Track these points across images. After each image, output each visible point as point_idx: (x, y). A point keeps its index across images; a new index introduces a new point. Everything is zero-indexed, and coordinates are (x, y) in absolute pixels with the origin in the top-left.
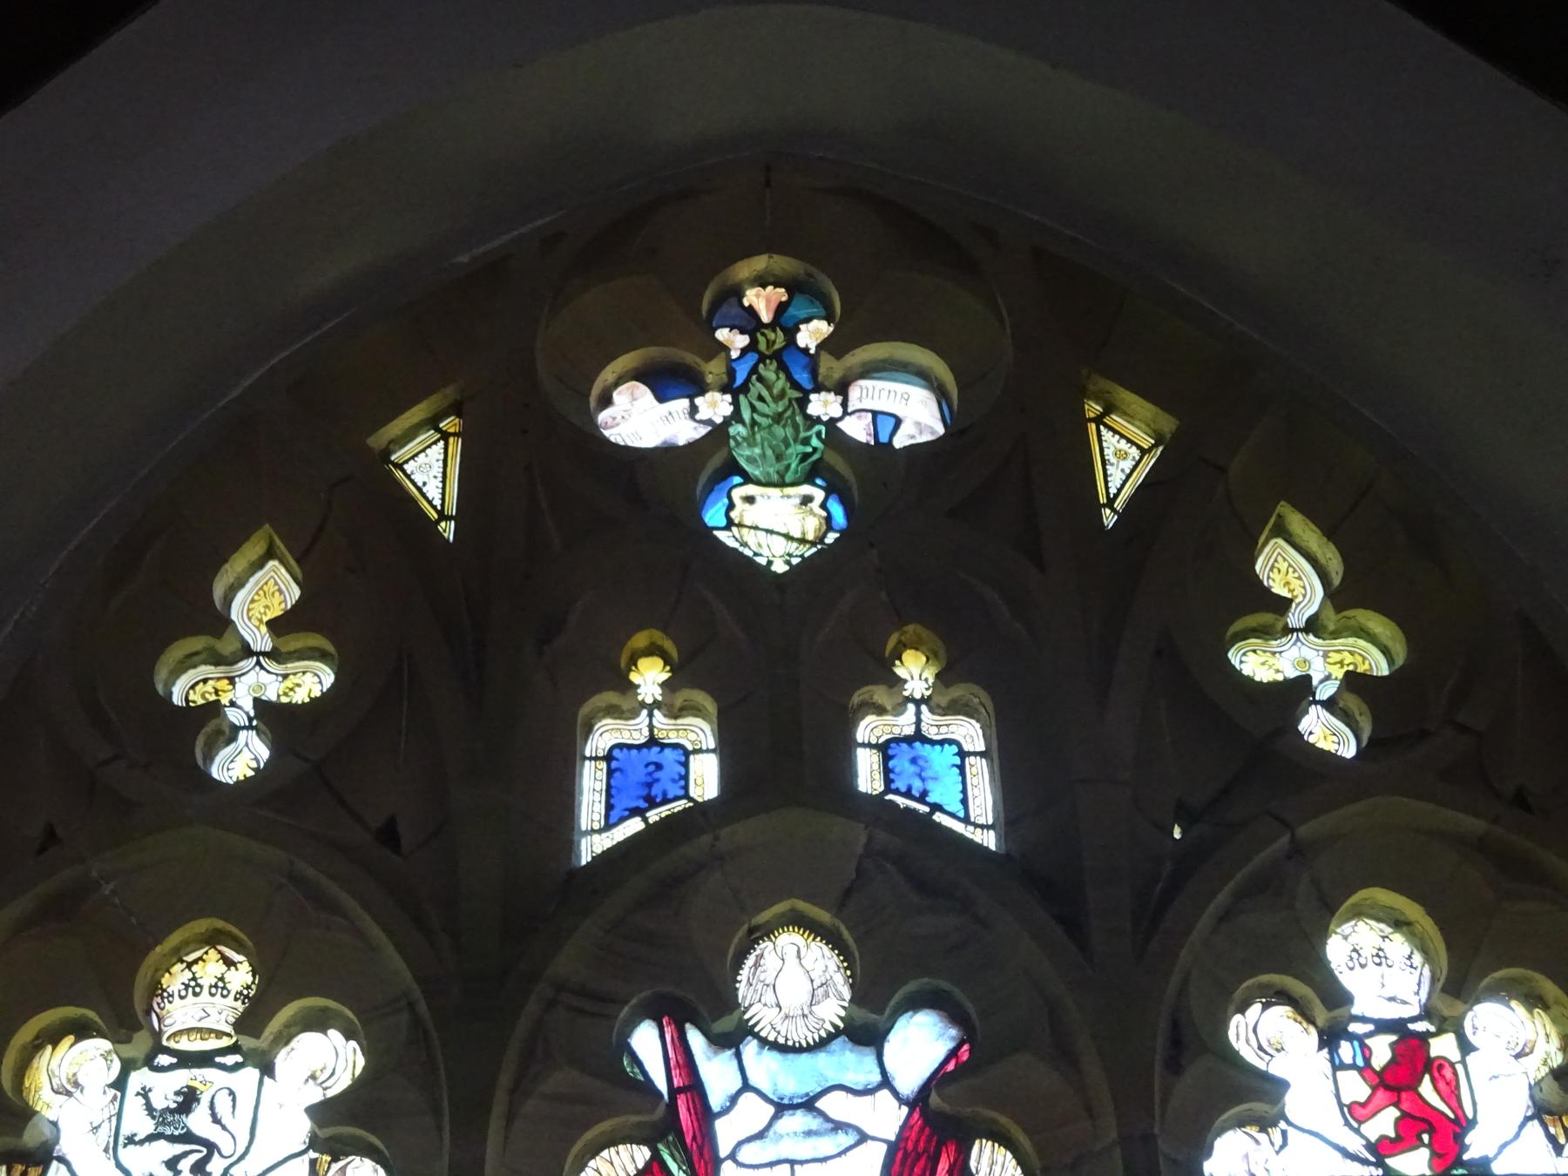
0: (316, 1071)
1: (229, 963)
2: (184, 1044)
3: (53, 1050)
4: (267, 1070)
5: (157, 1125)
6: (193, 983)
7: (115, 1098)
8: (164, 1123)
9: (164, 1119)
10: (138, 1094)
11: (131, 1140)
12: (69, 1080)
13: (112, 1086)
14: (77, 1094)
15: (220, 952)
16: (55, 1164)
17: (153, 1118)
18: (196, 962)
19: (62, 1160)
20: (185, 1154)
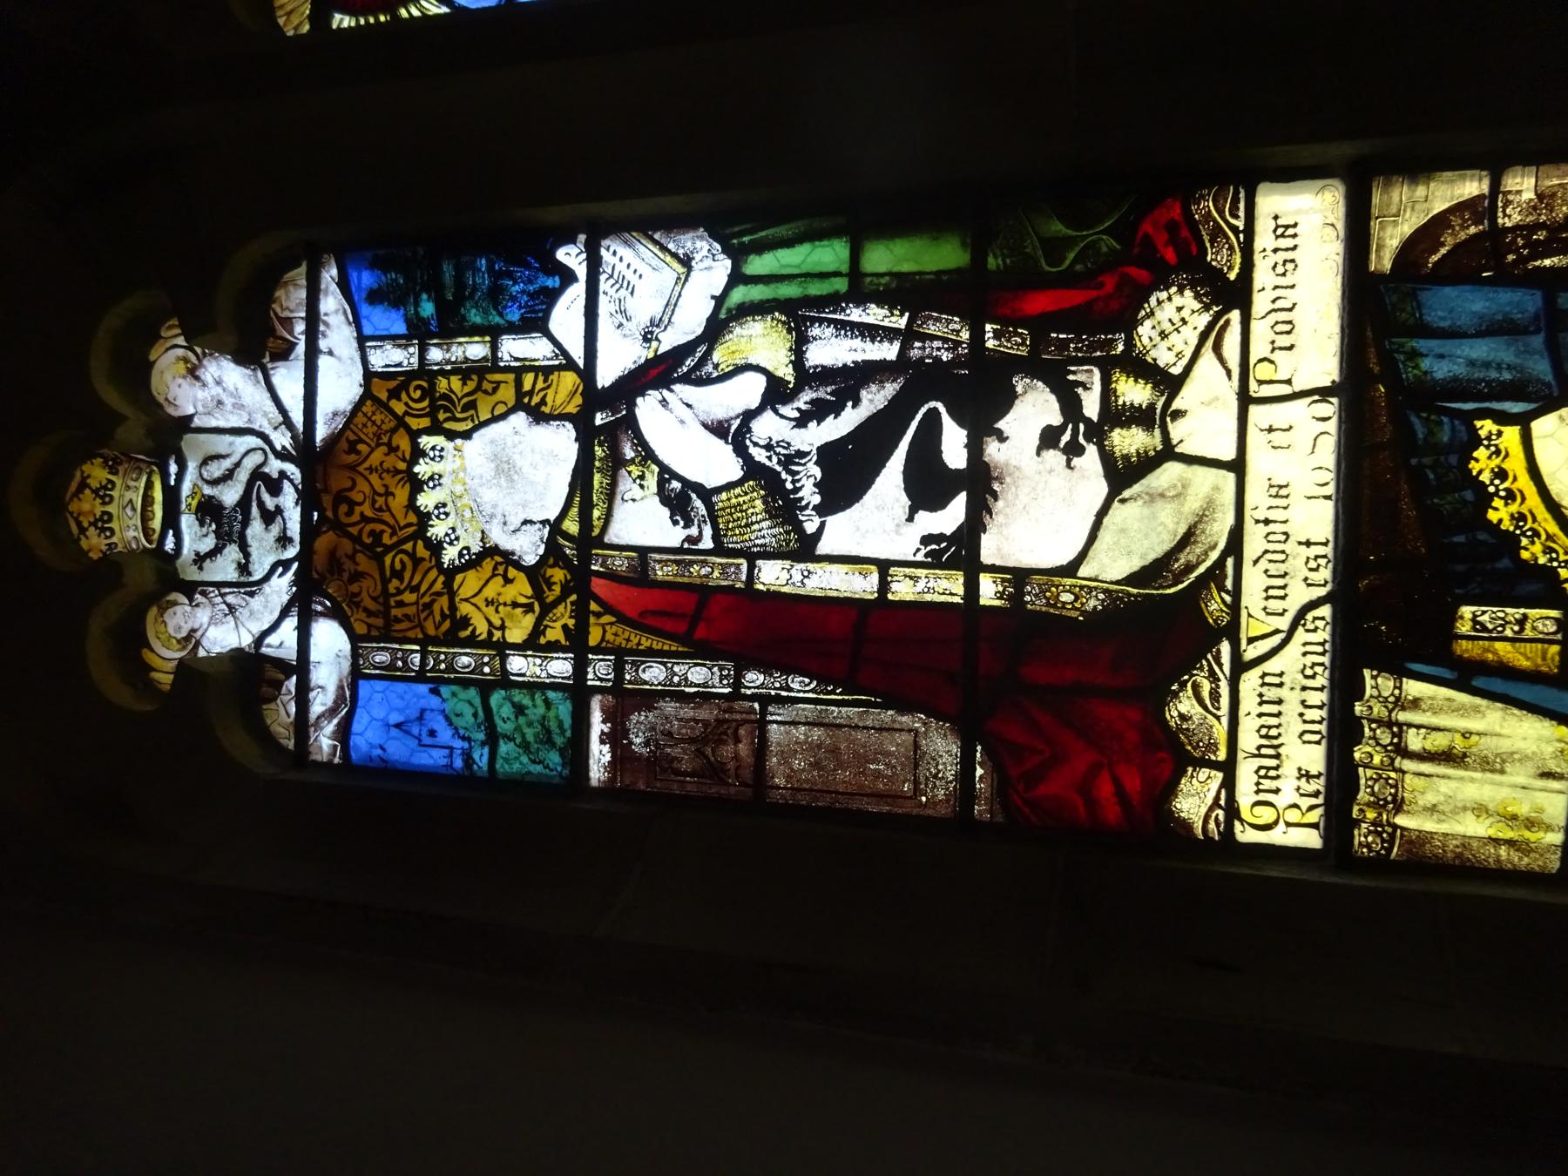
0: (187, 368)
1: (83, 485)
2: (157, 523)
3: (155, 670)
4: (184, 424)
5: (231, 541)
6: (100, 524)
7: (204, 594)
8: (230, 534)
9: (226, 535)
10: (201, 568)
11: (244, 568)
12: (184, 648)
13: (191, 599)
14: (199, 634)
15: (71, 499)
16: (264, 650)
17: (224, 546)
18: (79, 524)
19: (259, 640)
20: (261, 504)
